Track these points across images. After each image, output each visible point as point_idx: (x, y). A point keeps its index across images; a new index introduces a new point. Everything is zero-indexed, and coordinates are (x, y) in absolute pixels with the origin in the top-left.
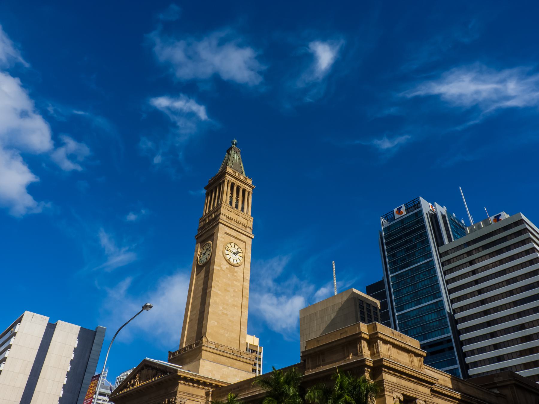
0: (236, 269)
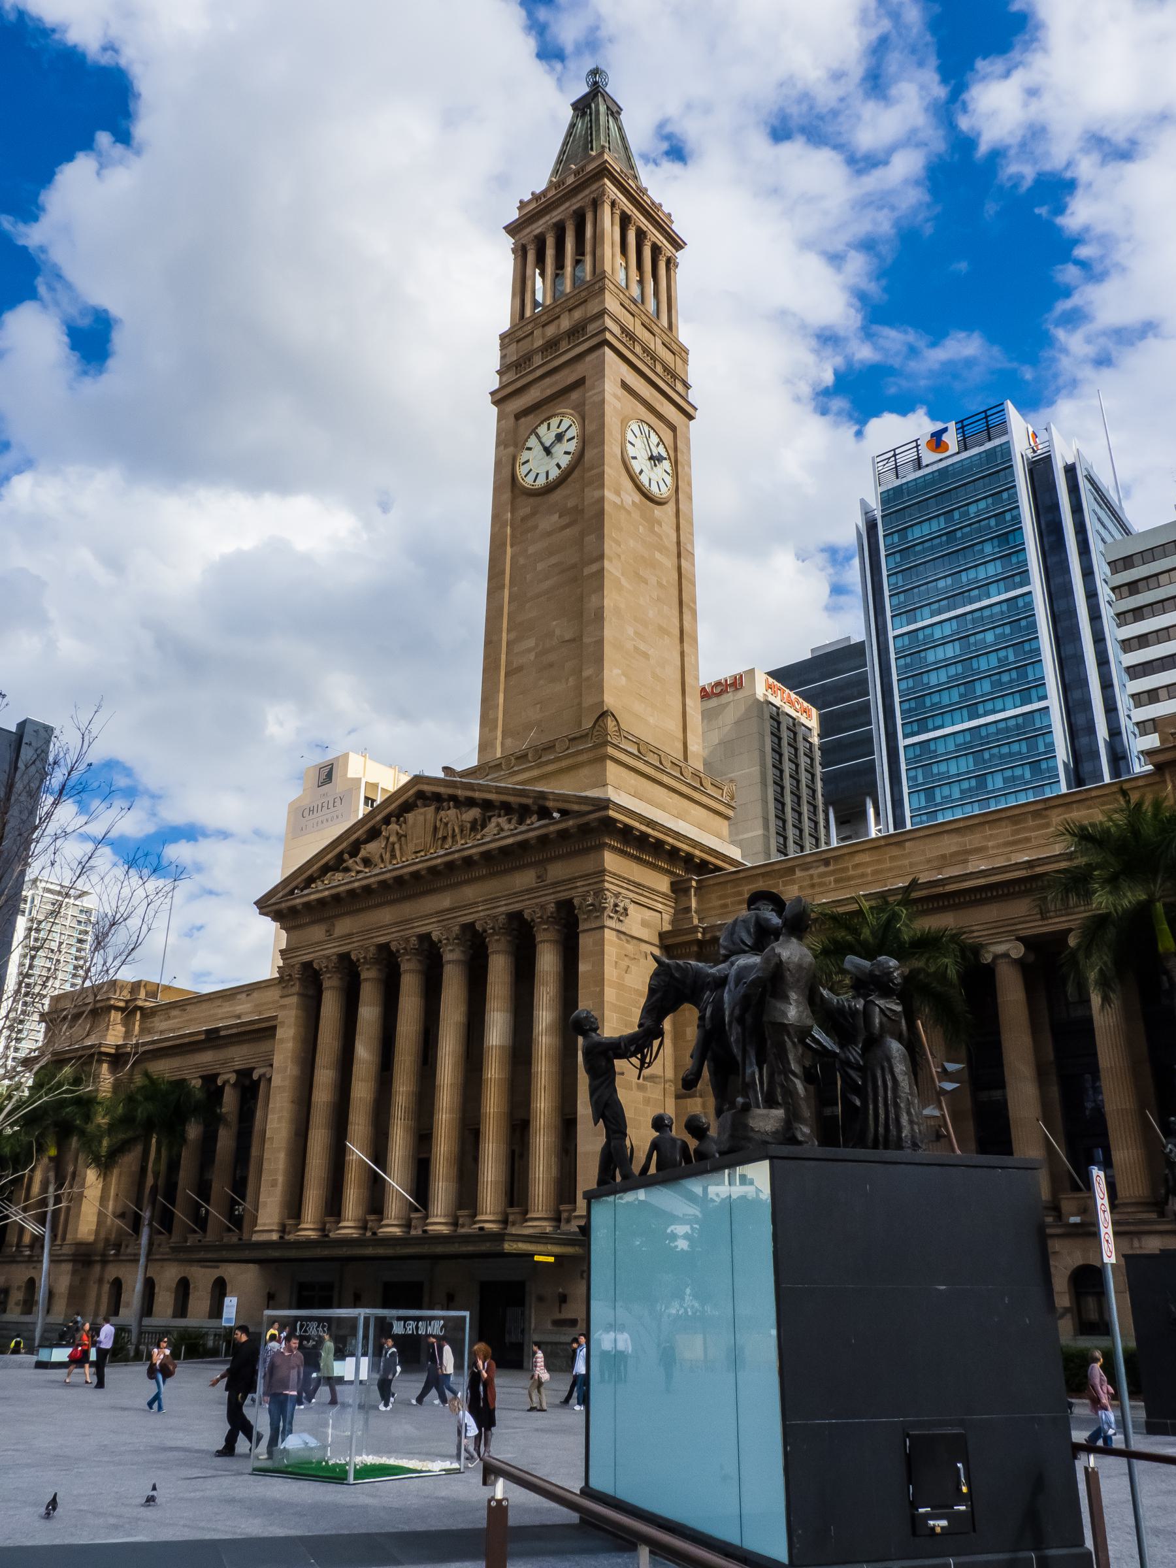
0: (658, 511)
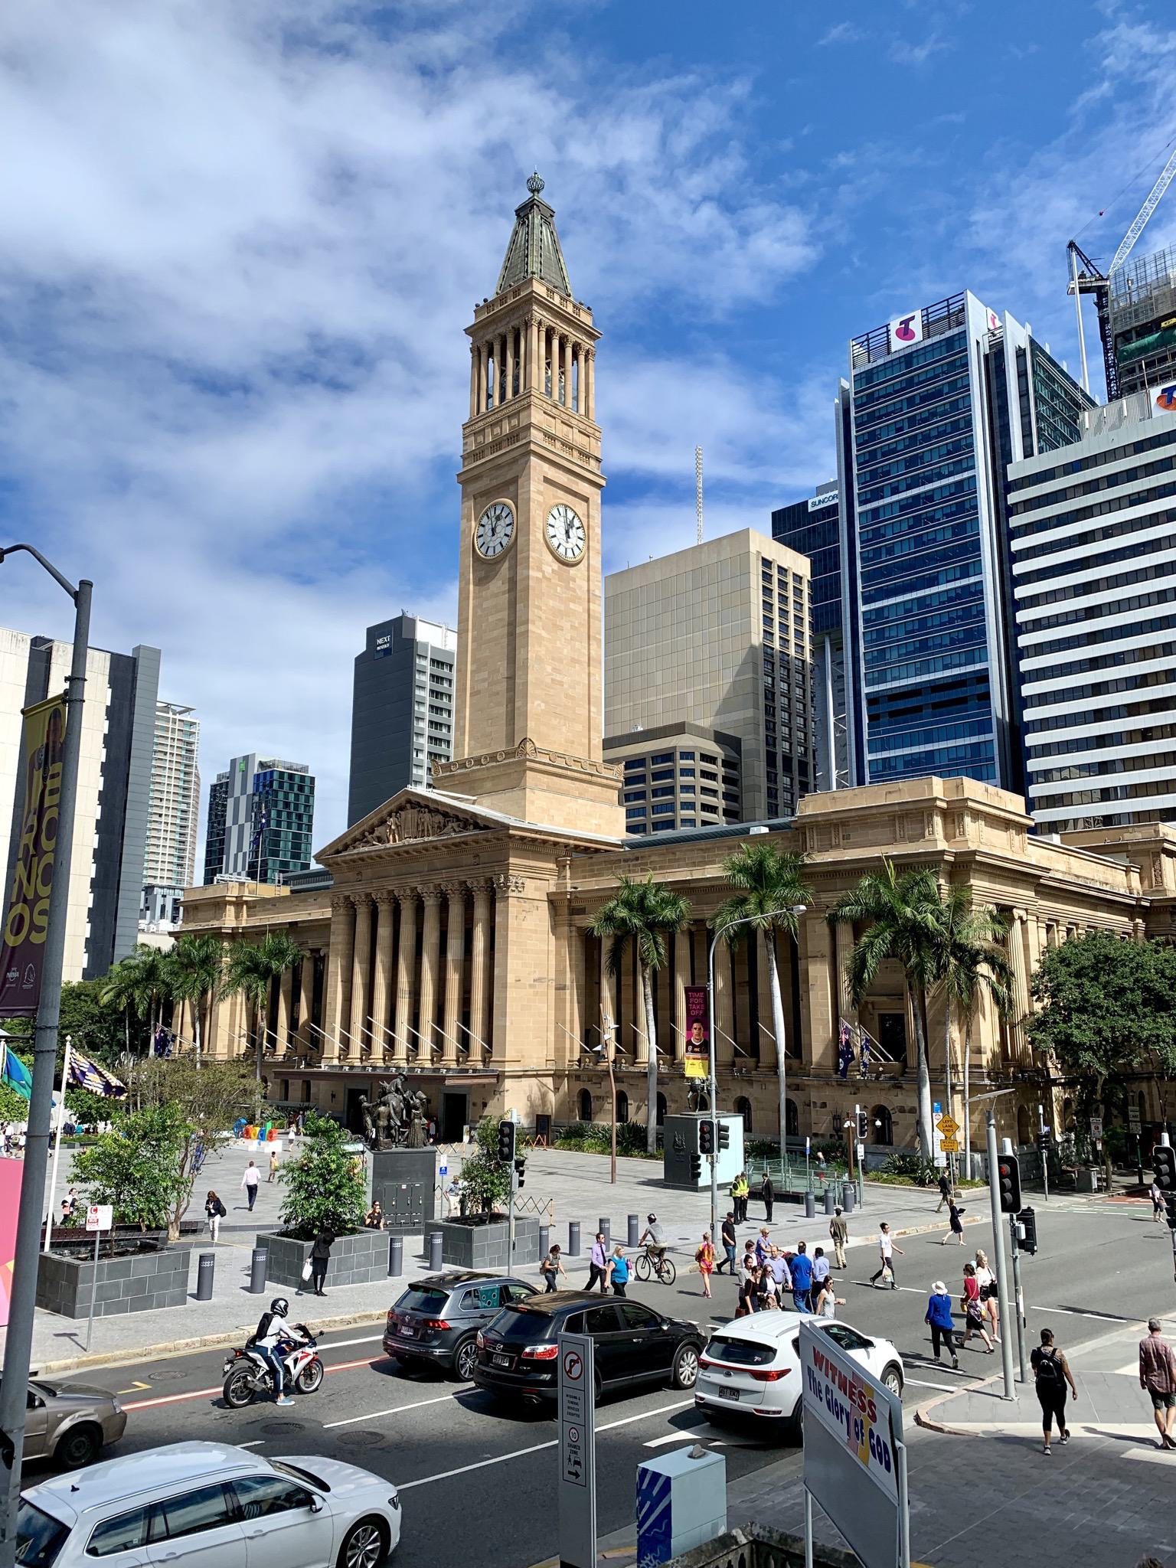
0: (572, 571)
